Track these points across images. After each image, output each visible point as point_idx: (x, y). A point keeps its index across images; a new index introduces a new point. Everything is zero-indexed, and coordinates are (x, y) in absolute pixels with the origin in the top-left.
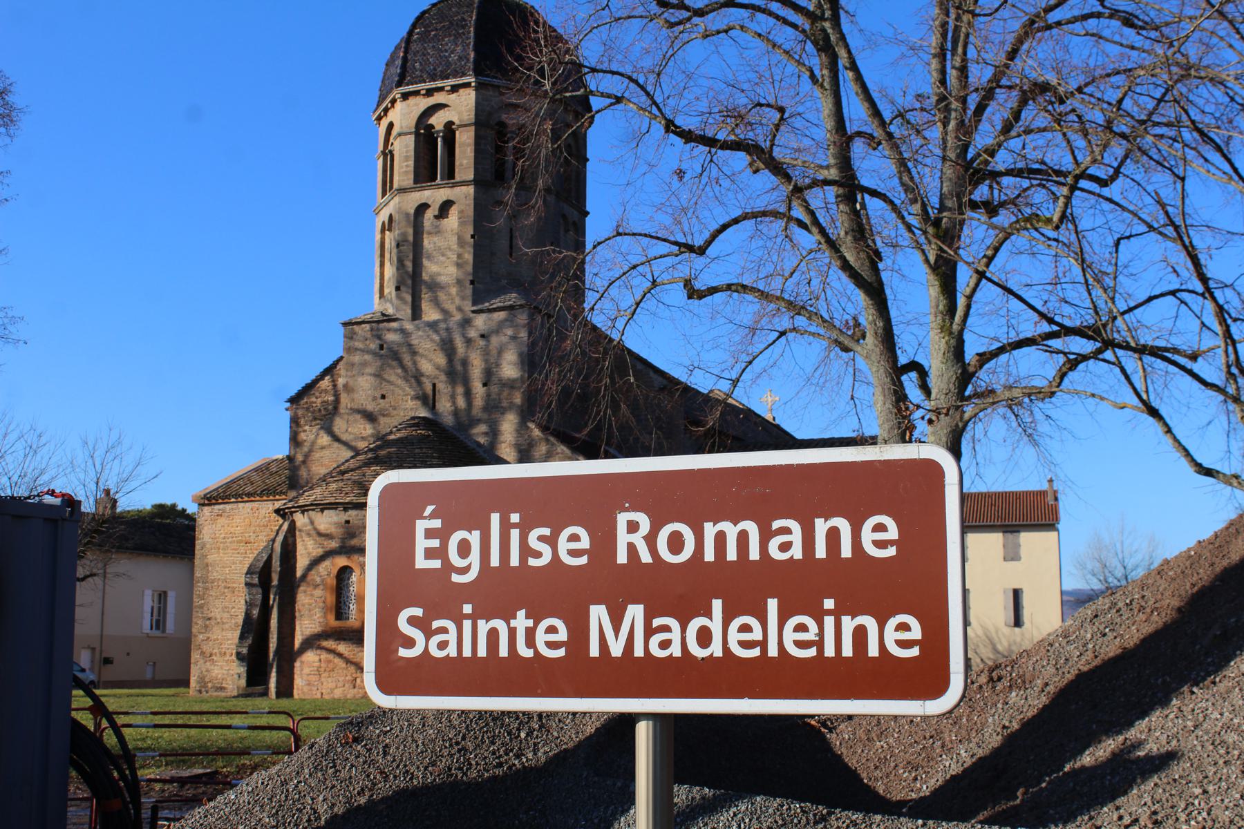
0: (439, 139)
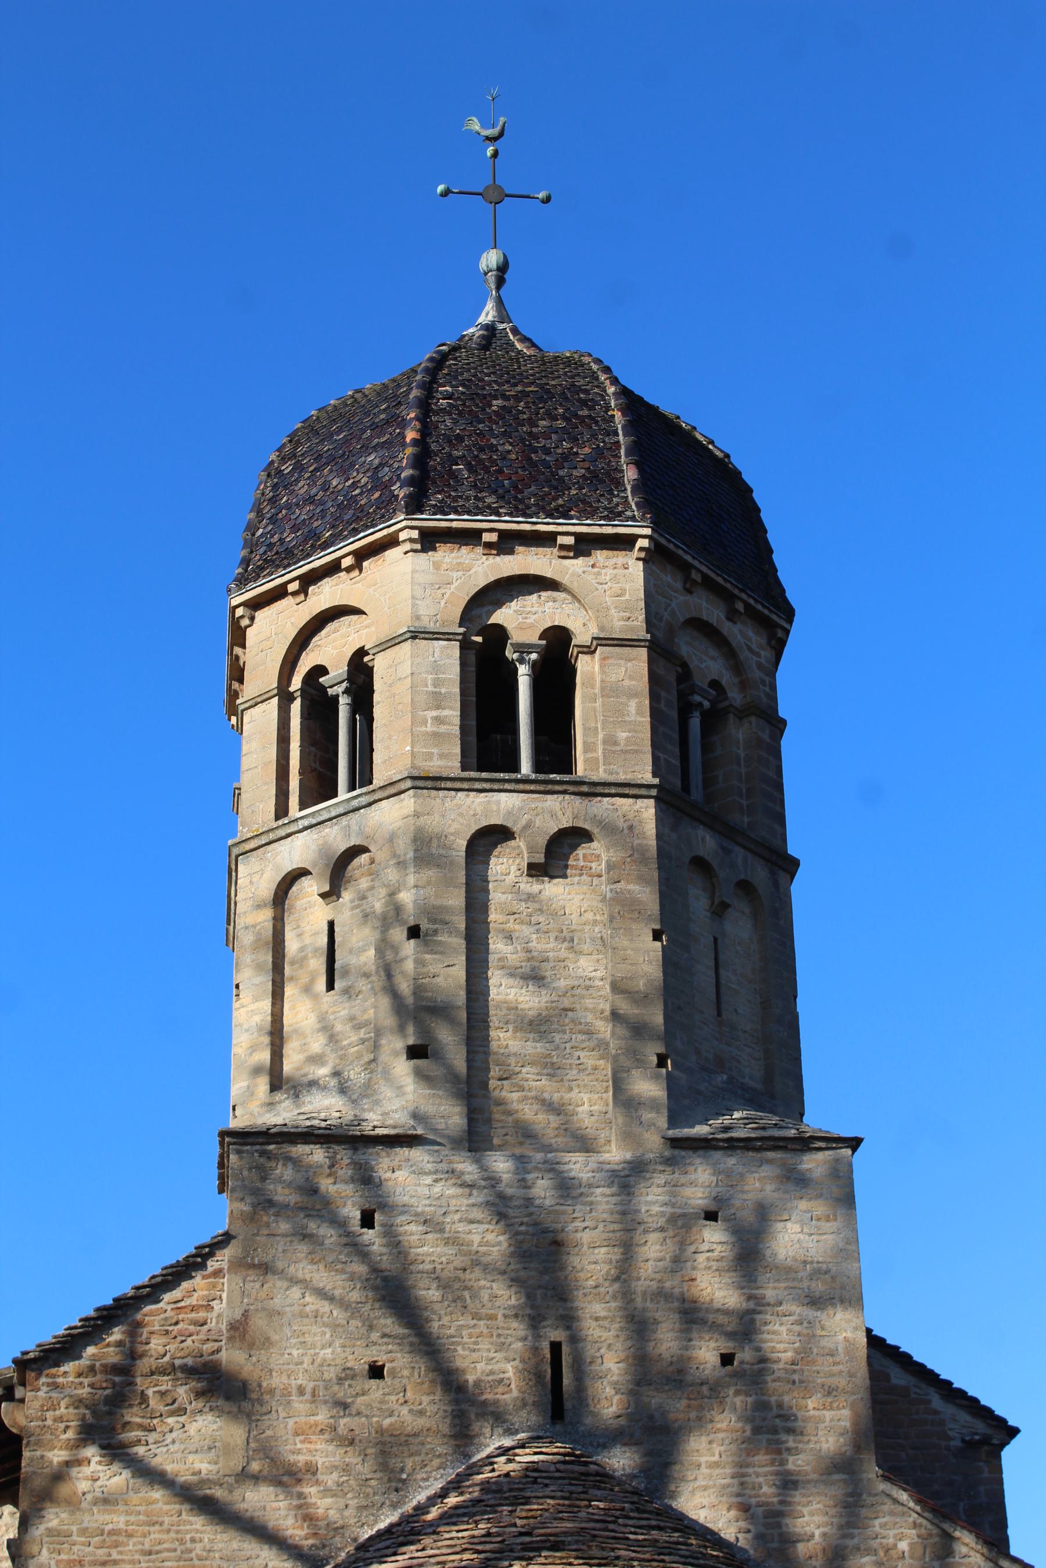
0: (523, 670)
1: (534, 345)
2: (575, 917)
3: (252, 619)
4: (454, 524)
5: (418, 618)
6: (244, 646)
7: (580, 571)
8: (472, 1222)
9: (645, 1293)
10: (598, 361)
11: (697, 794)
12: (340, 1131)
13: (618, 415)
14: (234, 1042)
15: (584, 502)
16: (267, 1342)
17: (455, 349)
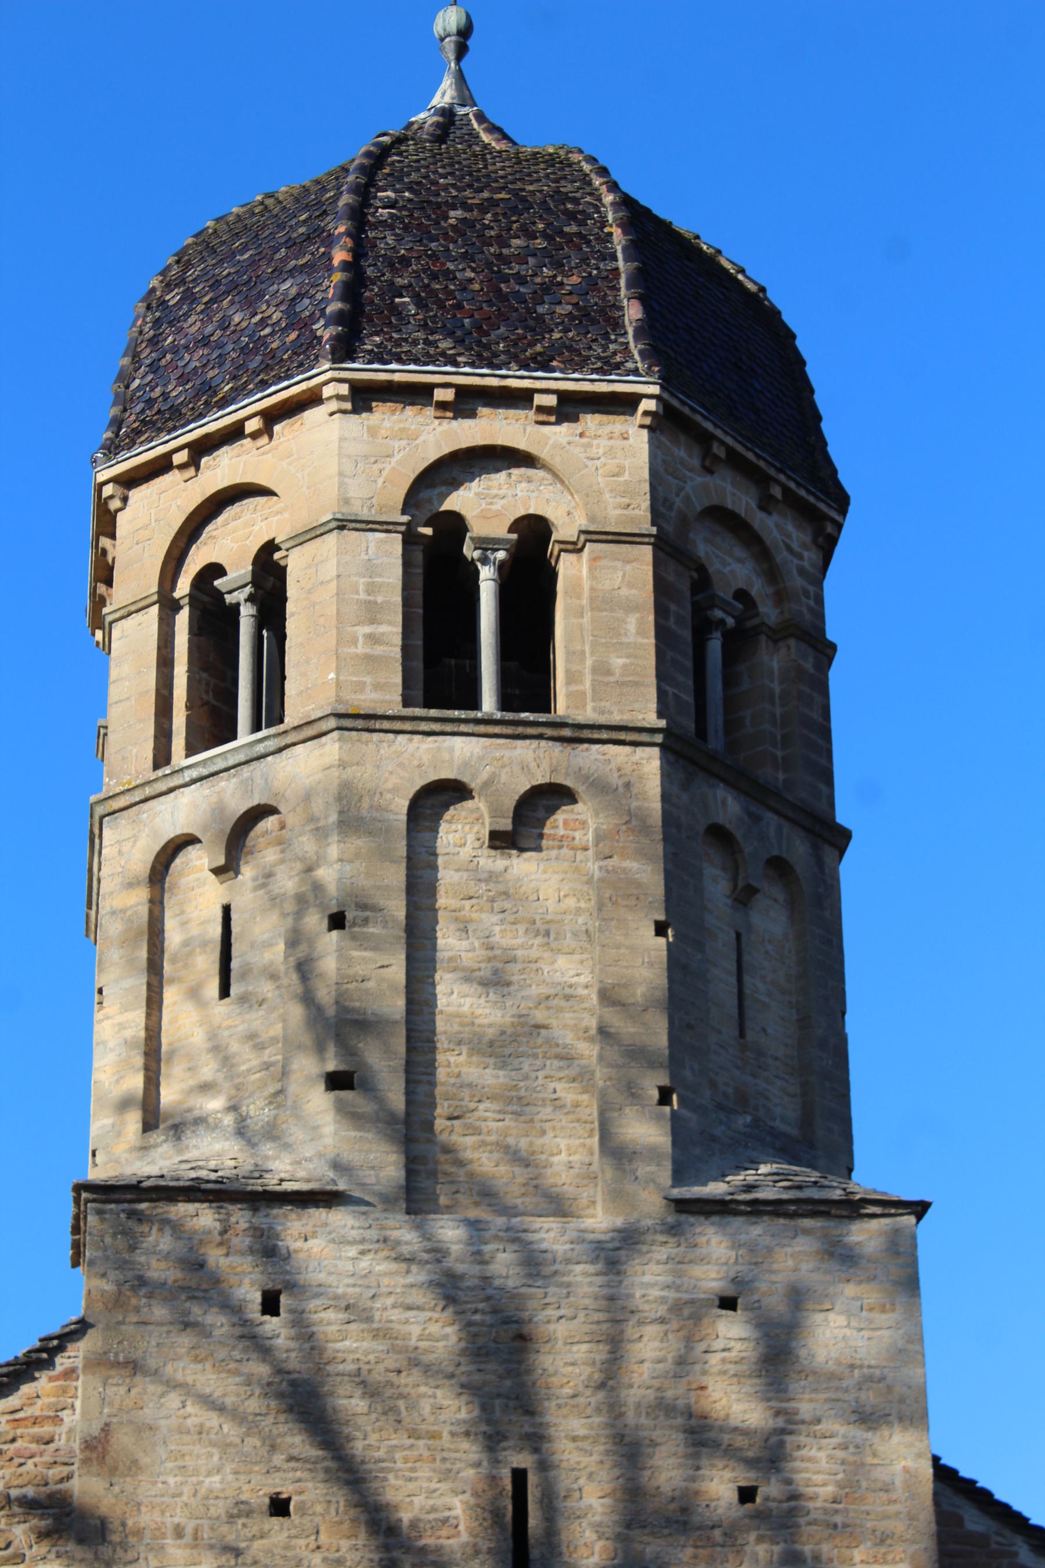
0: (487, 575)
1: (505, 137)
2: (551, 905)
3: (125, 500)
4: (397, 377)
5: (347, 501)
6: (113, 536)
7: (564, 441)
8: (409, 1308)
9: (638, 1405)
10: (591, 160)
11: (716, 742)
12: (235, 1186)
13: (617, 233)
14: (96, 1064)
15: (570, 349)
16: (134, 1467)
17: (400, 140)
